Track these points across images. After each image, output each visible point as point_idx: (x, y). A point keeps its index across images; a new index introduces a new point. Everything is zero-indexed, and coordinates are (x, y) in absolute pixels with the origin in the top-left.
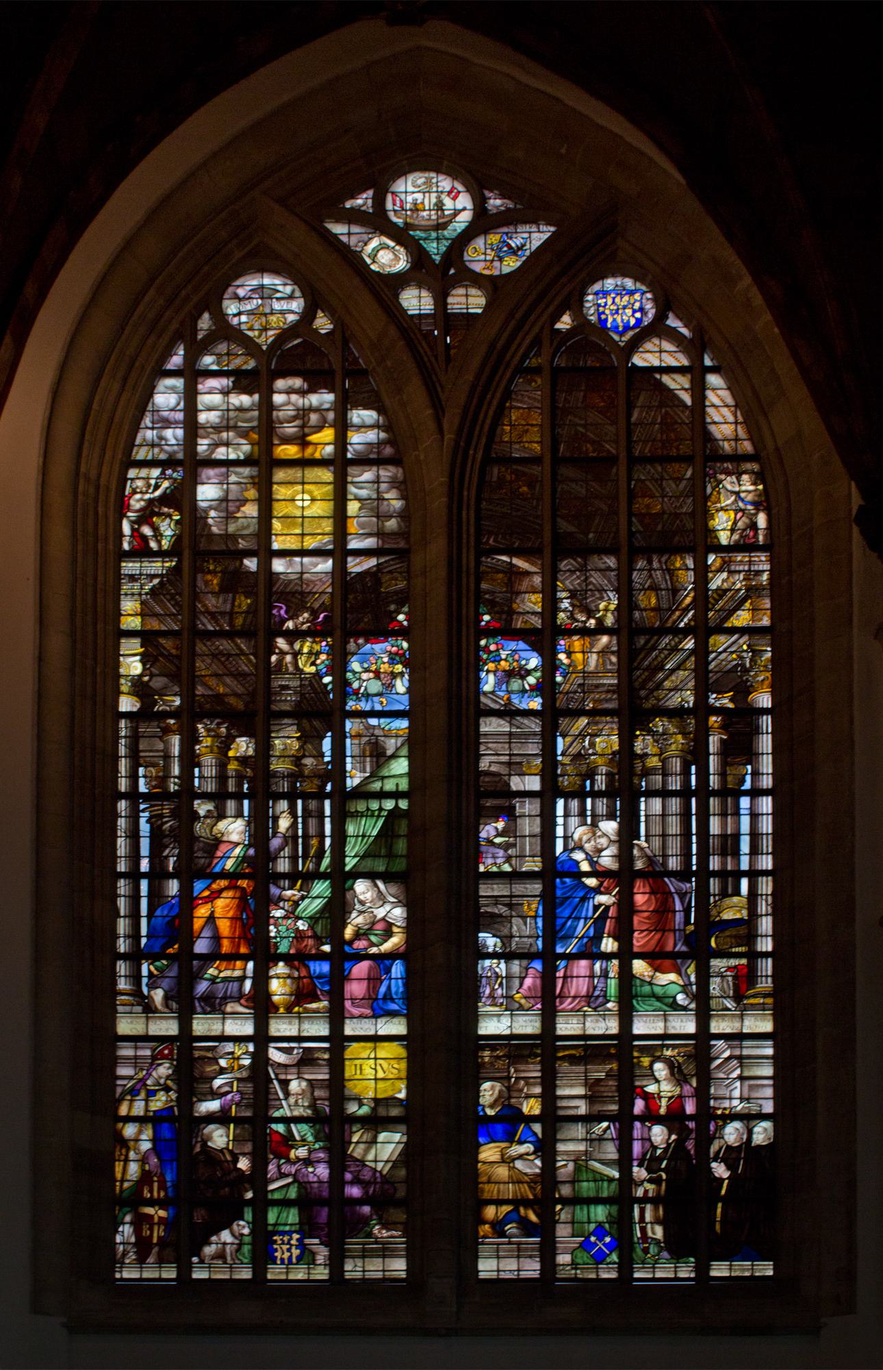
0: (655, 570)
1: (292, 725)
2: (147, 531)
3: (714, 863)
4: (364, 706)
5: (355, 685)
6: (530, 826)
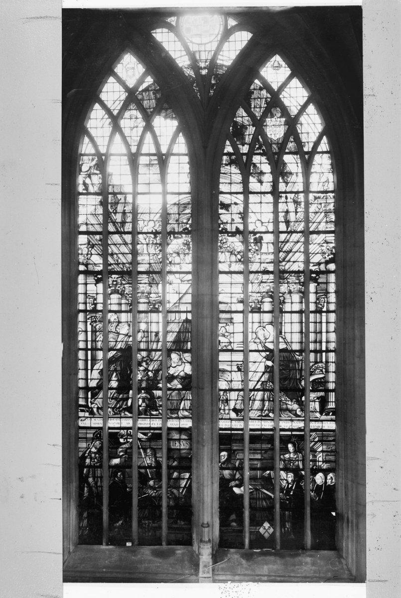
2: (88, 181)
3: (312, 346)
5: (170, 260)
6: (239, 328)
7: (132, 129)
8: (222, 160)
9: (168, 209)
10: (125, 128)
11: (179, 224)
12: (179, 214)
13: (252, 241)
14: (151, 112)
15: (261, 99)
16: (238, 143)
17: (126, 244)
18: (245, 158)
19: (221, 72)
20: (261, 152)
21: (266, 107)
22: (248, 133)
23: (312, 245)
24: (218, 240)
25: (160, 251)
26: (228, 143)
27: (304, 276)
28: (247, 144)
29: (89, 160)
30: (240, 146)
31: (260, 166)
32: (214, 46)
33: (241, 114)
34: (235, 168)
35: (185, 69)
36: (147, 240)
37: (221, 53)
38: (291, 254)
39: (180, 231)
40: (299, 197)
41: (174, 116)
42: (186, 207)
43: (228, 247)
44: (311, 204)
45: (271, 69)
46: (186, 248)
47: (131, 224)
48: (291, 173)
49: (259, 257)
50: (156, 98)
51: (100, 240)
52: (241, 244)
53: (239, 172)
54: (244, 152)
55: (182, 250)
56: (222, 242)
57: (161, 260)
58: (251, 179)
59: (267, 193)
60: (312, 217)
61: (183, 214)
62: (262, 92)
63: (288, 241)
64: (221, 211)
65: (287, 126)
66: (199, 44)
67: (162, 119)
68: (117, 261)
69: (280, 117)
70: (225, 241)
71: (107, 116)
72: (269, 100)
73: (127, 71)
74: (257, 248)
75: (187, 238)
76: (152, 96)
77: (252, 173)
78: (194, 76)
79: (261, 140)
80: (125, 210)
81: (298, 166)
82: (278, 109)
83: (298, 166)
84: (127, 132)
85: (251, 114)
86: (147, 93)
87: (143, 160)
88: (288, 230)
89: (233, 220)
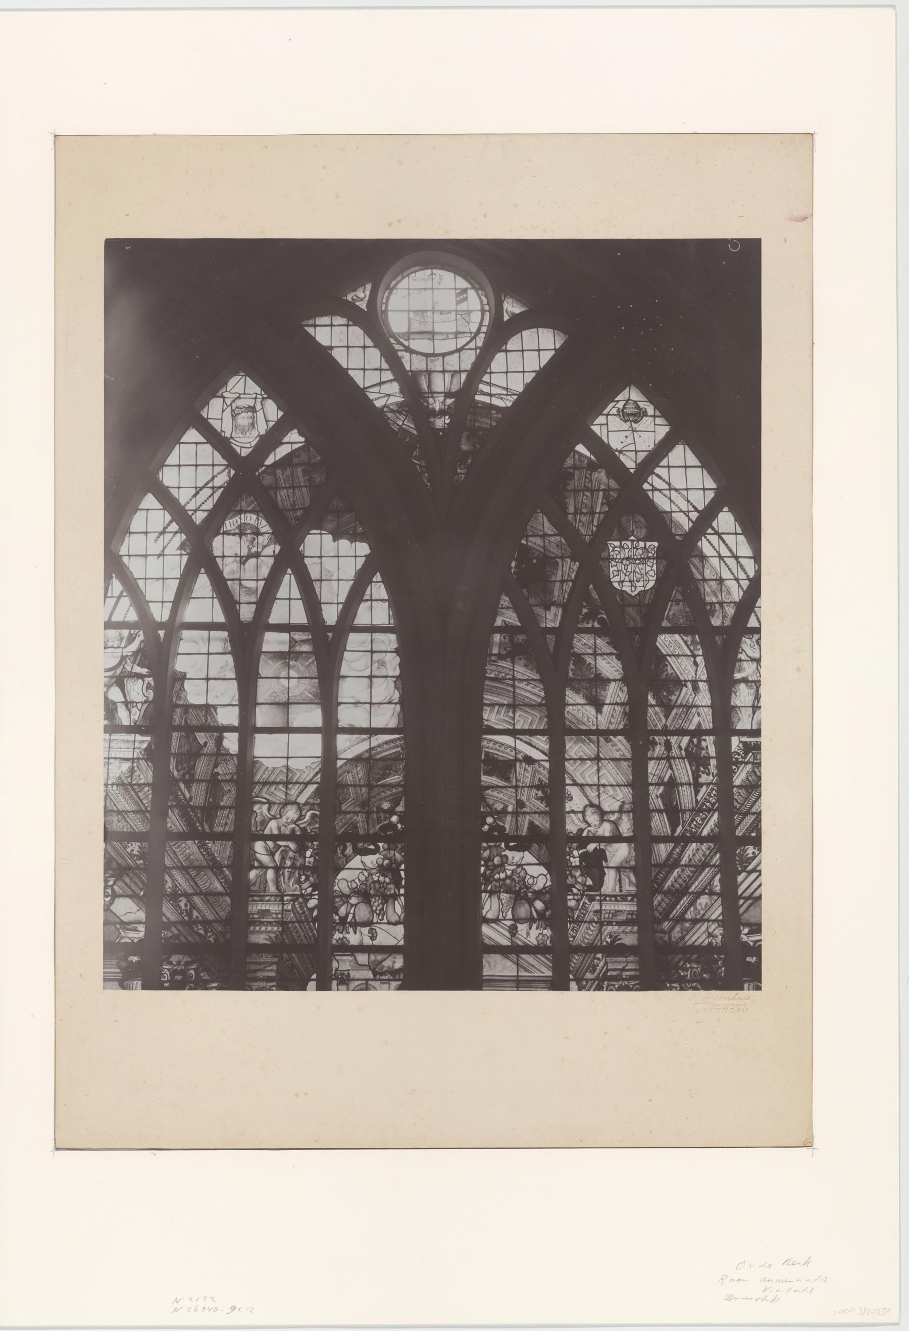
0: (674, 758)
1: (272, 964)
4: (353, 939)
5: (343, 911)
7: (243, 560)
8: (489, 644)
9: (340, 771)
10: (223, 557)
11: (368, 814)
12: (370, 787)
13: (575, 862)
14: (297, 518)
15: (592, 491)
16: (532, 601)
17: (215, 866)
18: (551, 639)
19: (485, 423)
20: (596, 625)
21: (605, 513)
22: (559, 578)
23: (744, 875)
24: (480, 858)
25: (314, 886)
26: (505, 600)
27: (724, 960)
28: (557, 605)
29: (122, 639)
30: (539, 610)
31: (593, 662)
32: (468, 359)
33: (541, 528)
34: (526, 666)
35: (389, 415)
36: (277, 857)
37: (486, 378)
38: (685, 901)
39: (371, 832)
40: (704, 744)
41: (360, 529)
42: (389, 768)
43: (507, 877)
44: (737, 763)
45: (617, 419)
46: (387, 880)
47: (233, 812)
48: (679, 683)
49: (595, 906)
50: (311, 485)
51: (142, 855)
52: (542, 870)
53: (537, 677)
54: (550, 625)
55: (377, 885)
56: (490, 863)
57: (315, 913)
58: (572, 697)
59: (616, 733)
60: (740, 799)
61: (383, 786)
62: (595, 475)
63: (676, 864)
64: (486, 779)
65: (664, 562)
66: (427, 355)
67: (328, 538)
68: (190, 914)
69: (645, 540)
70: (497, 860)
71: (174, 527)
72: (614, 494)
73: (234, 416)
74: (589, 882)
75: (392, 852)
76: (302, 480)
77: (572, 680)
78: (415, 432)
79: (595, 595)
80: (218, 774)
81: (696, 664)
82: (639, 518)
83: (696, 664)
84: (229, 568)
85: (563, 527)
86: (288, 472)
87: (273, 642)
88: (676, 835)
89: (520, 804)
